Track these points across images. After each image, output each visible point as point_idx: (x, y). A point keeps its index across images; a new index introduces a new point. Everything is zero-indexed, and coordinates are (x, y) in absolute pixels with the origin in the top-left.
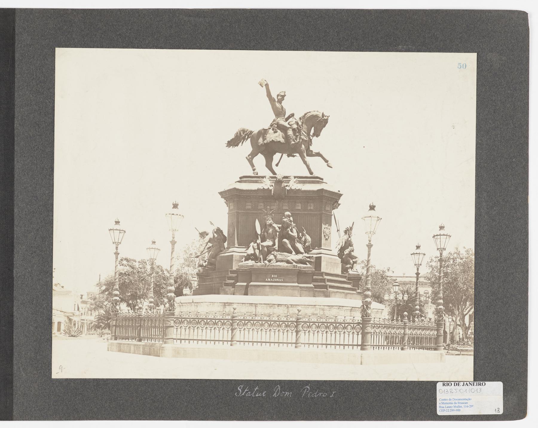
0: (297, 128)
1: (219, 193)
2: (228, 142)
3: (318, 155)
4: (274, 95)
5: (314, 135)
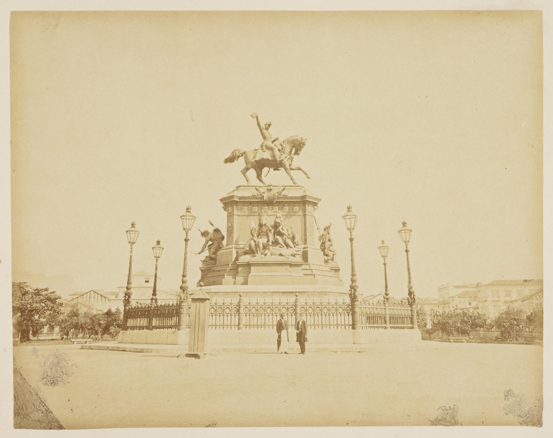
2: (226, 159)
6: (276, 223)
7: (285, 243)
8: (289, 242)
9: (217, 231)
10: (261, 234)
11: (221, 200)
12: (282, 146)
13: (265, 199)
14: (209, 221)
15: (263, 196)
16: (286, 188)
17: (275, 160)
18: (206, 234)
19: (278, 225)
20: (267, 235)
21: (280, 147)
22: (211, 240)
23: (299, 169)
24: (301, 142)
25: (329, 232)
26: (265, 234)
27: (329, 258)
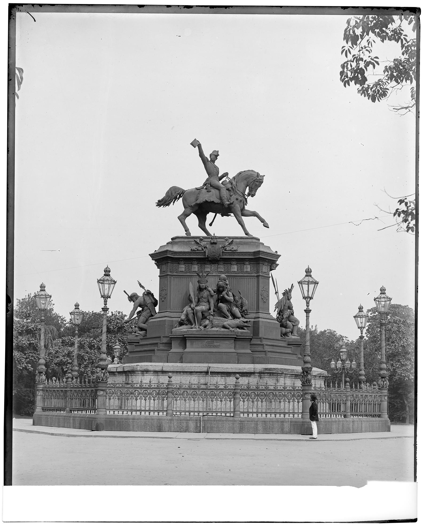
0: (232, 188)
1: (149, 255)
2: (159, 201)
3: (255, 214)
4: (207, 155)
5: (249, 195)
6: (219, 287)
7: (230, 311)
8: (236, 310)
9: (149, 294)
10: (200, 300)
11: (151, 255)
12: (232, 184)
13: (207, 256)
14: (138, 282)
15: (205, 252)
16: (235, 240)
17: (222, 204)
18: (134, 299)
19: (221, 289)
20: (209, 302)
21: (229, 186)
22: (140, 306)
23: (255, 214)
24: (256, 179)
25: (289, 298)
26: (205, 300)
27: (288, 330)
